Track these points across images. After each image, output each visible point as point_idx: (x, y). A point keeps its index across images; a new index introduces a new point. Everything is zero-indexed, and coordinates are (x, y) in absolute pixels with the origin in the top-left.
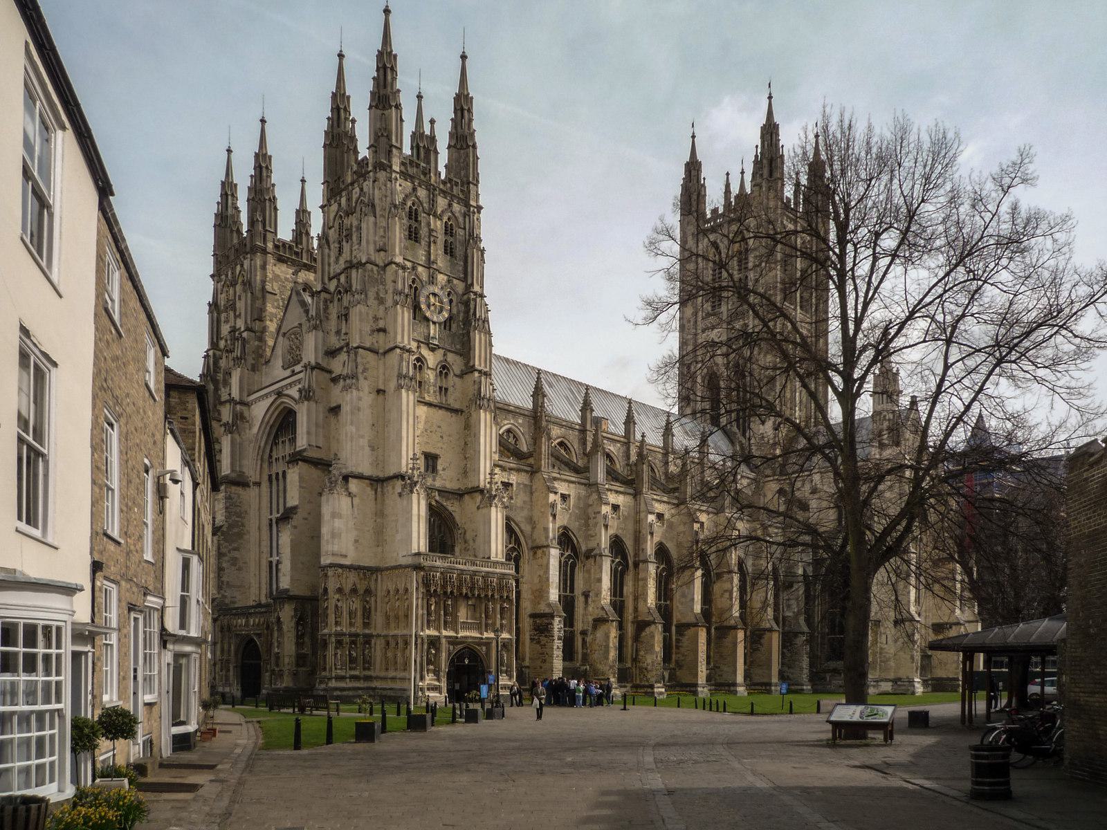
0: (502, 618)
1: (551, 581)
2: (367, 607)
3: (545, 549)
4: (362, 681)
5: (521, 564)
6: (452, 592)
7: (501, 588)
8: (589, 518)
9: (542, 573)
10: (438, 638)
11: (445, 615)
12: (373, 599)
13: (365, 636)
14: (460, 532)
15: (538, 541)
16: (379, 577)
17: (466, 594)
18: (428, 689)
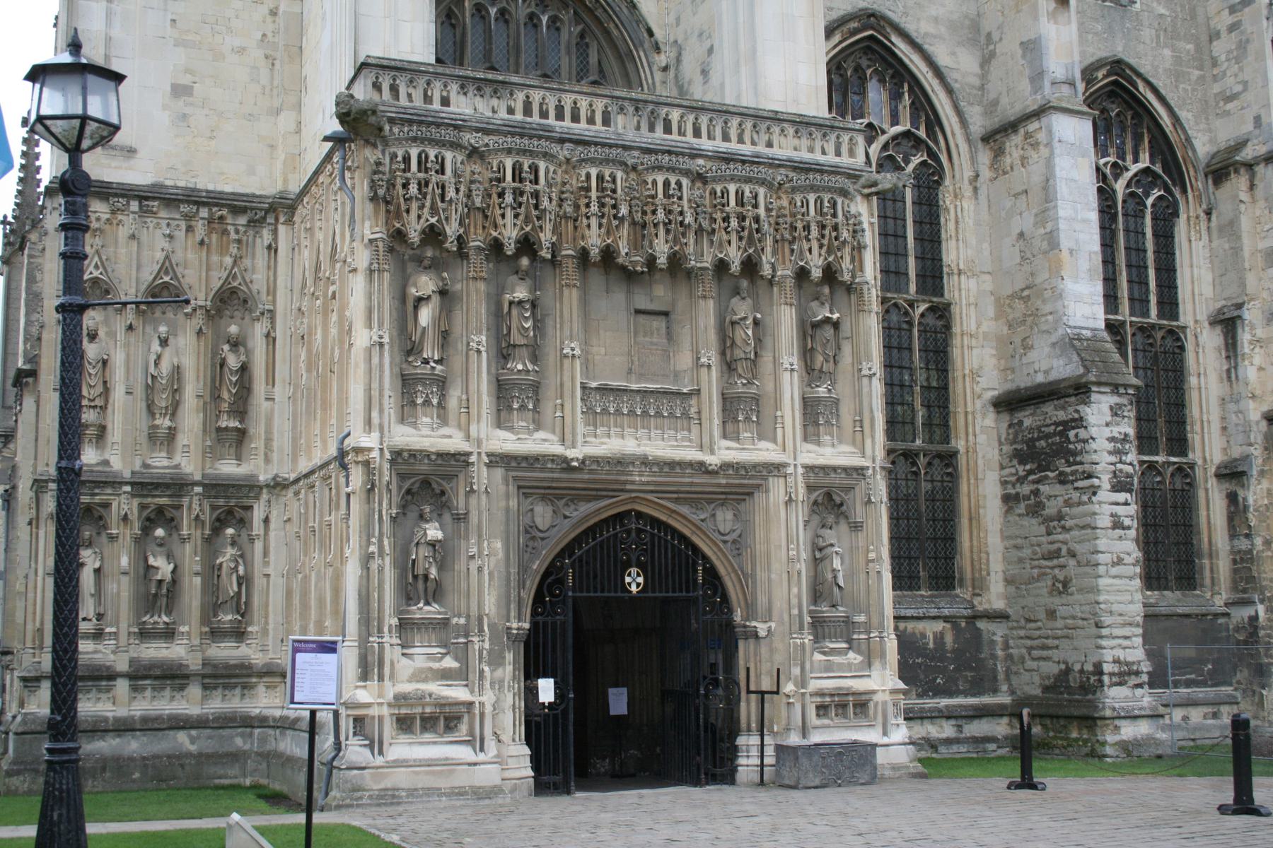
0: (811, 373)
1: (1065, 243)
2: (233, 362)
3: (1033, 126)
4: (195, 690)
5: (946, 198)
6: (527, 245)
7: (789, 234)
8: (1214, 36)
9: (1025, 222)
10: (460, 459)
11: (504, 353)
12: (259, 329)
13: (215, 487)
14: (662, 60)
15: (1004, 101)
16: (282, 229)
17: (608, 254)
18: (404, 724)
